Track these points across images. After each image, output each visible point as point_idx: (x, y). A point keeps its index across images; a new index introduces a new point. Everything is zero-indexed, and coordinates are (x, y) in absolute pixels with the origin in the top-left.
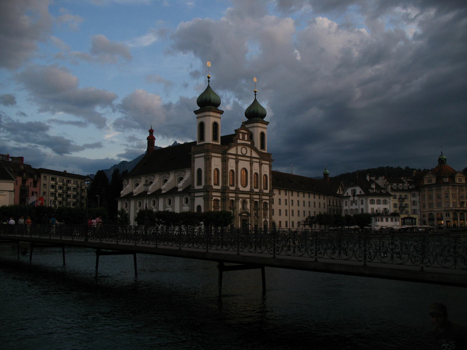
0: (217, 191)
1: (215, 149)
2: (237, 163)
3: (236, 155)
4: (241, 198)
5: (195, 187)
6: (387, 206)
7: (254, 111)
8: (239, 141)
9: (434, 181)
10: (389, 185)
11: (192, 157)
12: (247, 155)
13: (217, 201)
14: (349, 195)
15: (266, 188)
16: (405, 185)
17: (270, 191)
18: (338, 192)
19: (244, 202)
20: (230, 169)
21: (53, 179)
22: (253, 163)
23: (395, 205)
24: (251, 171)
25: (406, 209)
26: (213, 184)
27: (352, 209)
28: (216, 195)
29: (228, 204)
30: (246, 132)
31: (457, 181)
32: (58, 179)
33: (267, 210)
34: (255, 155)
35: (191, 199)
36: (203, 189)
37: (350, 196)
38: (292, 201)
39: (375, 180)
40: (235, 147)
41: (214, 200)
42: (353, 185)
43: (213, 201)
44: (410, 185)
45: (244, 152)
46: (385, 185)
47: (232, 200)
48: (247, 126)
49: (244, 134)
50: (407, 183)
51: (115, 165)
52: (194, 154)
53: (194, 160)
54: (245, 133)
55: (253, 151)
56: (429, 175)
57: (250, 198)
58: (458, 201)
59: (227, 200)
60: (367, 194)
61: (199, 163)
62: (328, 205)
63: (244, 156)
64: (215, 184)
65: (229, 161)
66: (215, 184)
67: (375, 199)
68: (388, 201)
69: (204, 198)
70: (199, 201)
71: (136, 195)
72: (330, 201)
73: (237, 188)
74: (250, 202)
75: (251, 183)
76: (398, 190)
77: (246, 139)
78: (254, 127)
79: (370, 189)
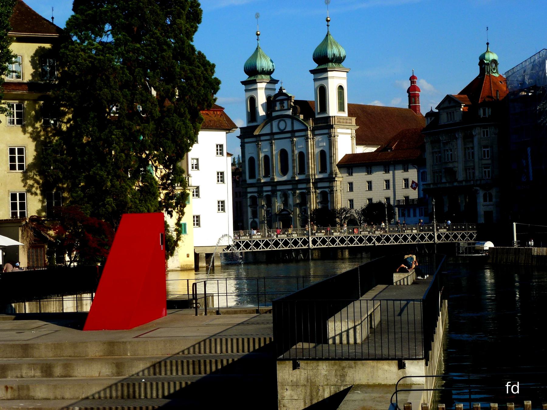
0: (252, 185)
3: (272, 134)
4: (279, 190)
8: (274, 114)
12: (286, 130)
13: (253, 198)
24: (293, 151)
33: (328, 203)
40: (269, 124)
41: (251, 197)
43: (249, 199)
55: (296, 121)
63: (282, 132)
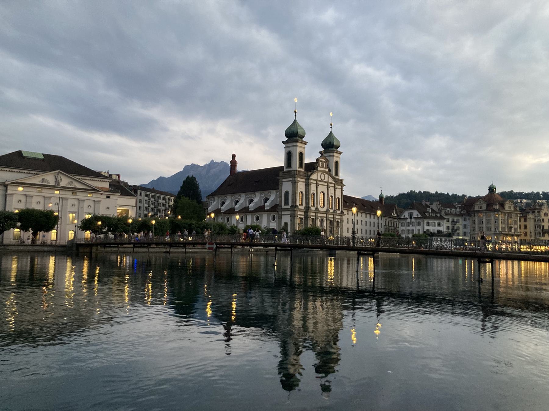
0: (301, 210)
1: (301, 175)
2: (317, 186)
3: (317, 180)
4: (320, 217)
5: (282, 206)
6: (441, 229)
7: (330, 143)
9: (484, 207)
10: (443, 209)
11: (280, 180)
12: (325, 180)
13: (301, 219)
14: (406, 217)
15: (339, 209)
16: (458, 210)
17: (341, 211)
18: (392, 215)
19: (322, 221)
20: (312, 192)
21: (147, 195)
22: (329, 188)
23: (448, 228)
24: (328, 194)
25: (458, 231)
26: (298, 205)
27: (408, 230)
28: (301, 214)
29: (310, 222)
30: (325, 161)
31: (506, 208)
32: (151, 195)
33: (339, 228)
34: (331, 180)
35: (279, 217)
36: (291, 208)
37: (407, 218)
38: (357, 220)
39: (430, 205)
41: (299, 218)
42: (411, 208)
44: (462, 210)
45: (323, 178)
46: (439, 209)
47: (313, 219)
48: (325, 155)
49: (323, 162)
50: (459, 208)
51: (184, 182)
52: (282, 179)
53: (282, 184)
54: (324, 162)
56: (480, 202)
57: (326, 217)
58: (506, 226)
59: (309, 218)
60: (424, 217)
61: (286, 186)
62: (384, 226)
63: (322, 181)
64: (300, 205)
65: (311, 185)
66: (300, 205)
67: (431, 221)
68: (442, 223)
69: (290, 216)
70: (286, 219)
71: (224, 211)
72: (386, 222)
73: (317, 209)
74: (327, 221)
75: (327, 204)
76: (451, 214)
77: (325, 167)
78: (330, 156)
79: (426, 212)
